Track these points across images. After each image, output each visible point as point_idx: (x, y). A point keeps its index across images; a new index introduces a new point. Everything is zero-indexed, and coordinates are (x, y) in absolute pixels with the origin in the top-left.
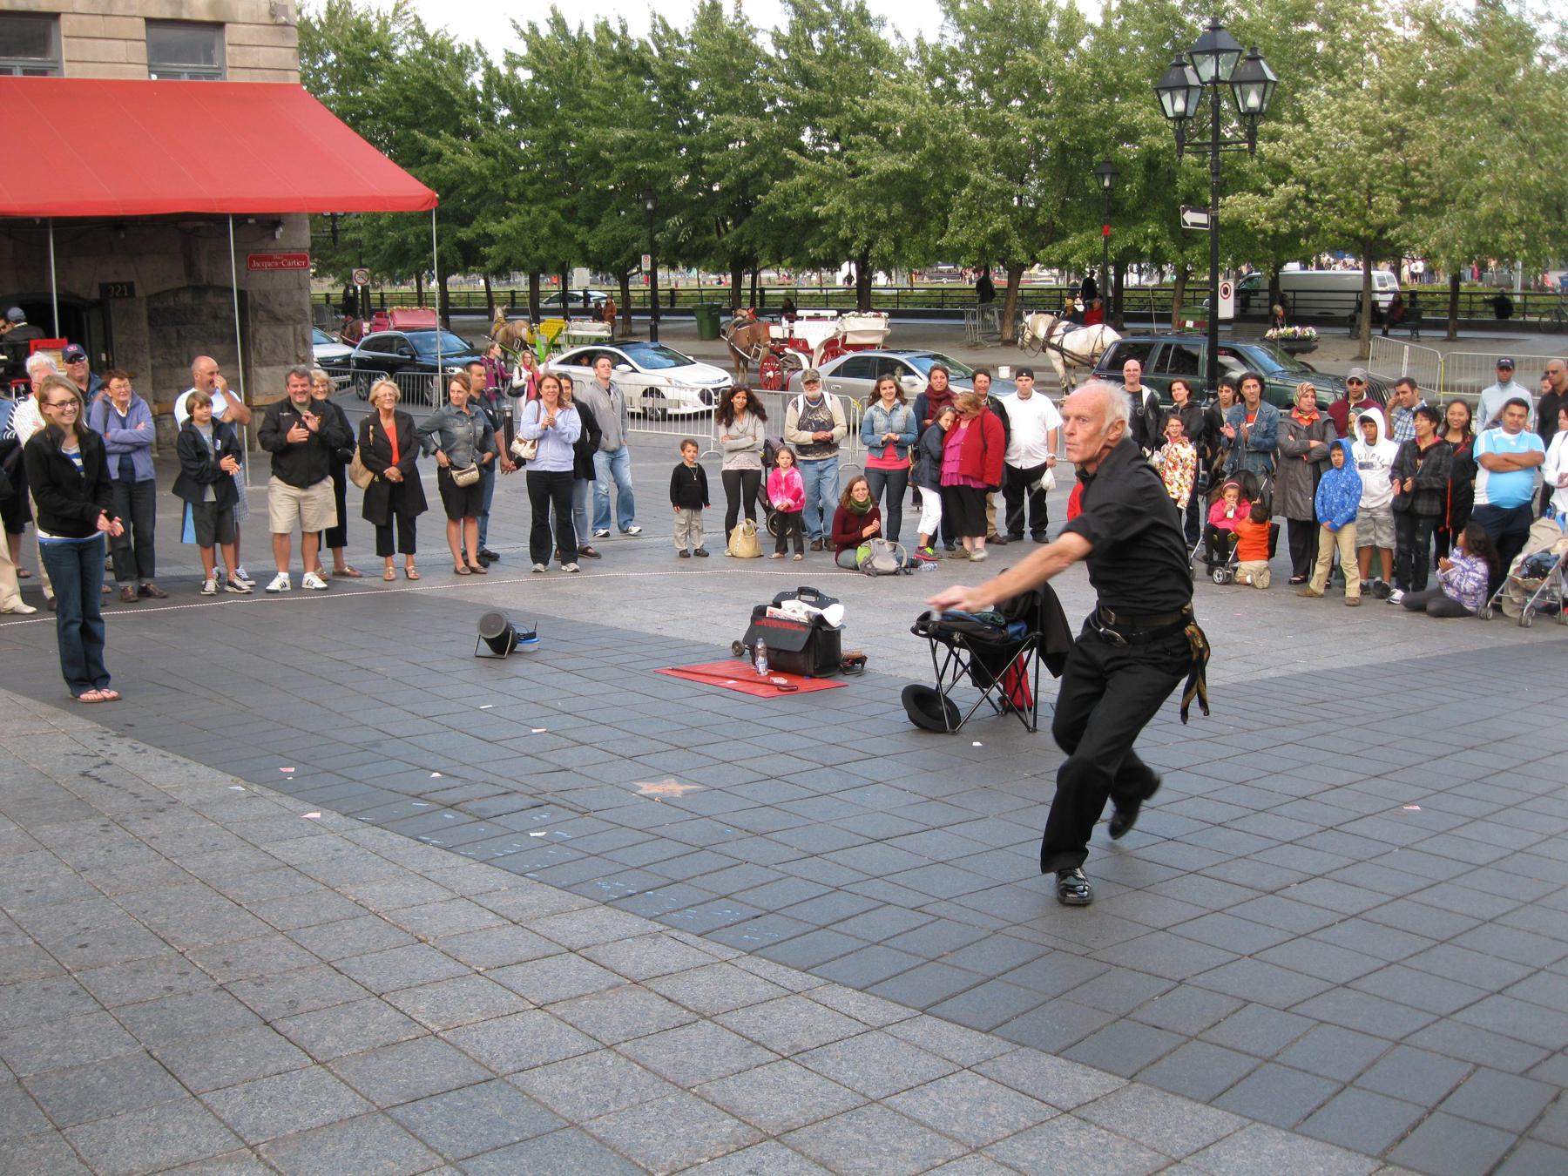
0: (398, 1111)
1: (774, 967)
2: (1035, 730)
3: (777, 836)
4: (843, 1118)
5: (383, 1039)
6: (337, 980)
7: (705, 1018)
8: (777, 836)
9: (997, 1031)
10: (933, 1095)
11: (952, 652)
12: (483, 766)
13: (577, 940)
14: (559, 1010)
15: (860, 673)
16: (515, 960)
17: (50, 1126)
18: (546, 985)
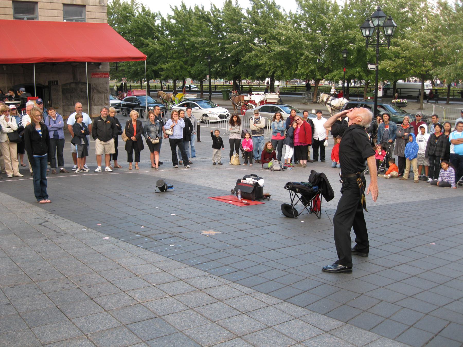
0: (129, 326)
1: (241, 286)
2: (320, 218)
3: (243, 247)
4: (260, 332)
5: (125, 305)
6: (112, 287)
8: (243, 247)
9: (306, 307)
10: (287, 326)
12: (157, 225)
13: (183, 277)
14: (177, 297)
15: (269, 200)
16: (165, 282)
17: (27, 327)
18: (173, 290)
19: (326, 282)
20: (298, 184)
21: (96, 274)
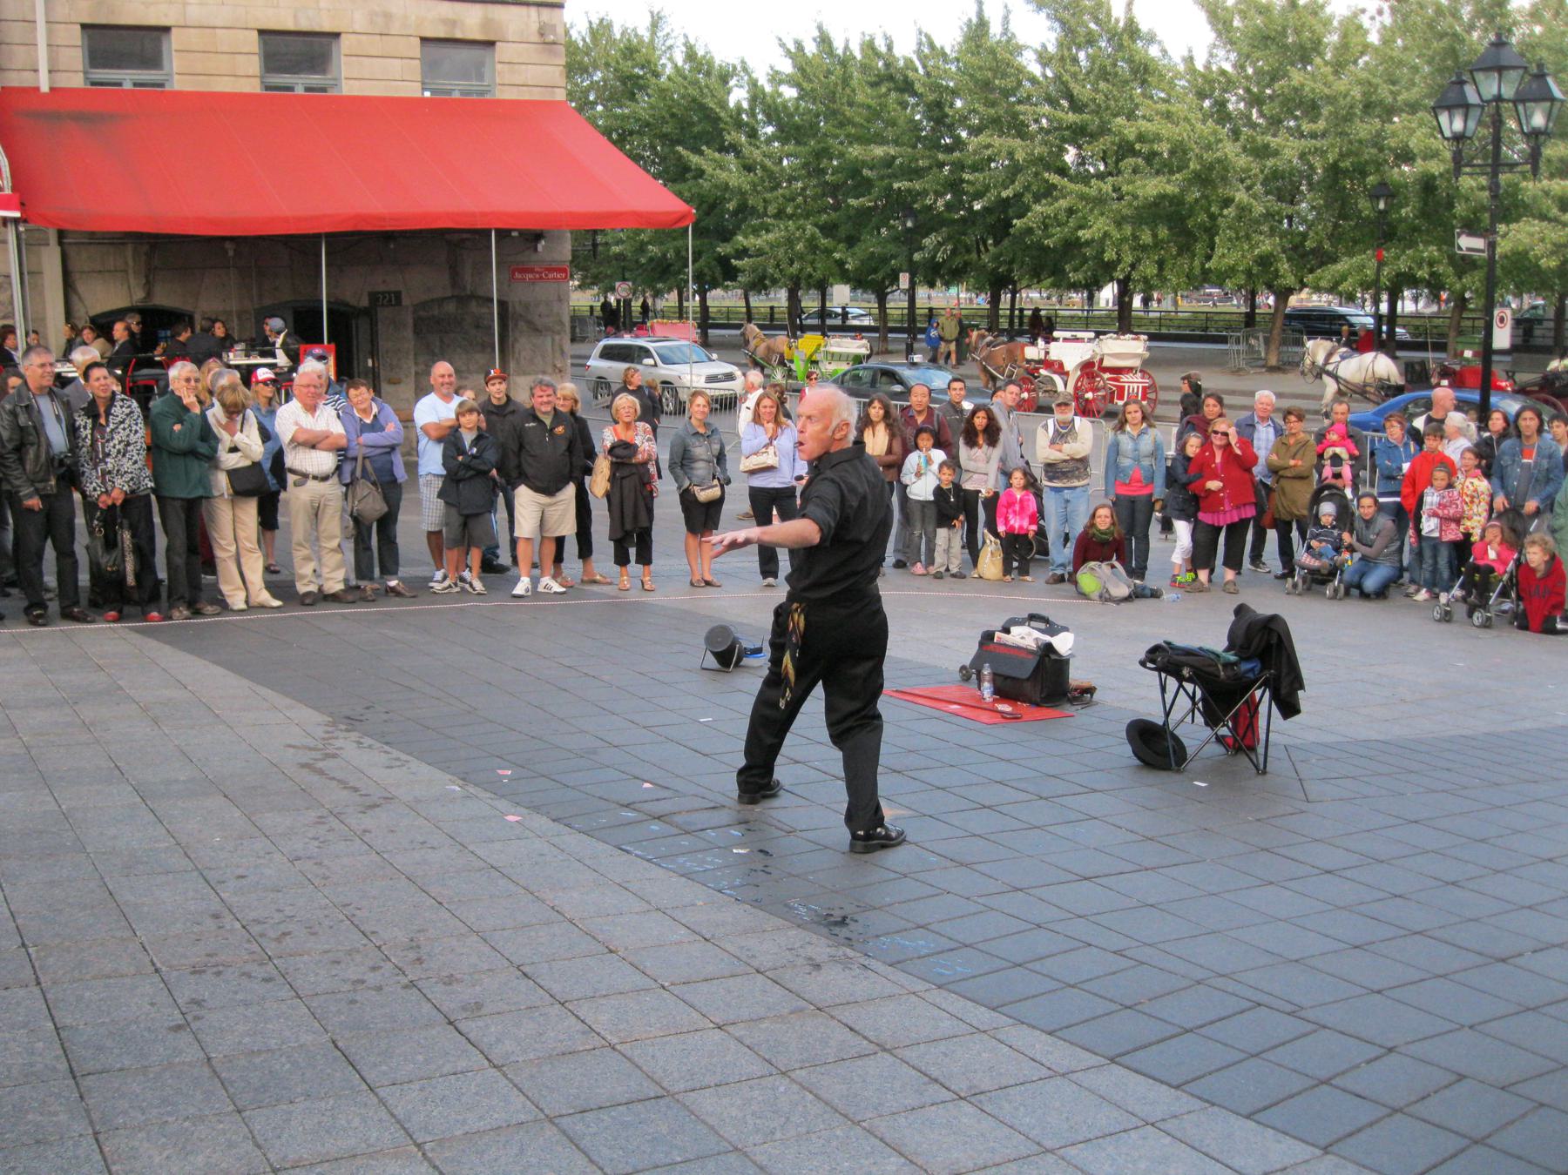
0: (564, 1122)
1: (962, 1002)
2: (1264, 772)
7: (885, 1050)
11: (1181, 686)
14: (738, 1031)
15: (1089, 704)
17: (232, 1107)
19: (1264, 999)
20: (1188, 652)
21: (475, 938)
